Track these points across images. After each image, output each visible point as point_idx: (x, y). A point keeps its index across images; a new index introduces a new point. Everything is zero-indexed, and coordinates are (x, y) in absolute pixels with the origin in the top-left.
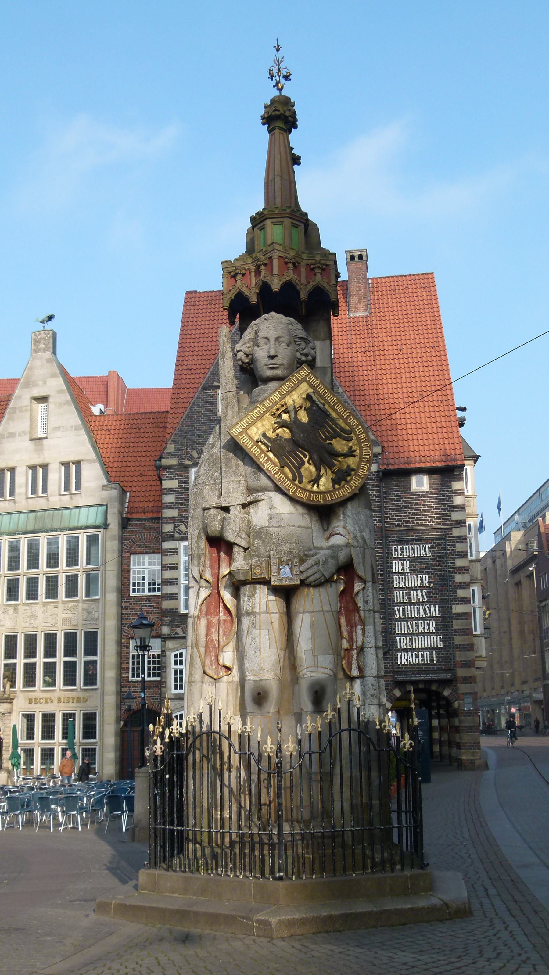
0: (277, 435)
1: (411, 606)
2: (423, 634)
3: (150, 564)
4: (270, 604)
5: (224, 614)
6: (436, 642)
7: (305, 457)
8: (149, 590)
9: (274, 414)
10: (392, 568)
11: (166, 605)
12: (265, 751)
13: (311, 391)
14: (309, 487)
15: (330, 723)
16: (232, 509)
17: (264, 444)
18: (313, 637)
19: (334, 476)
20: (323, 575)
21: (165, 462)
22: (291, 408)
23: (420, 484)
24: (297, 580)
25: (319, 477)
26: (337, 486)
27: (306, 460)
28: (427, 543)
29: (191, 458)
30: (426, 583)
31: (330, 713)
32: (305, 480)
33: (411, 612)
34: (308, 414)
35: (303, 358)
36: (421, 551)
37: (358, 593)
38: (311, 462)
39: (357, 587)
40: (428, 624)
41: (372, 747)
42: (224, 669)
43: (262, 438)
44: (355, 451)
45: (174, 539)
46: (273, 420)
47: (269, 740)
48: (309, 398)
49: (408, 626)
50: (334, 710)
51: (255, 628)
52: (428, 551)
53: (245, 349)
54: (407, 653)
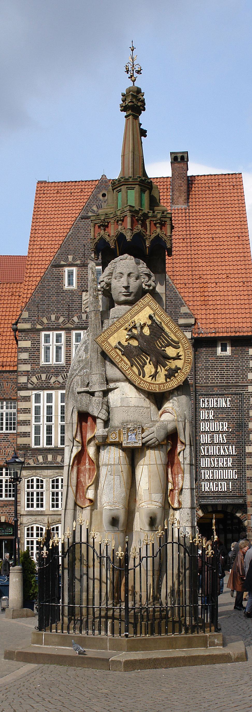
0: (129, 343)
1: (213, 446)
2: (222, 468)
3: (7, 408)
4: (121, 458)
5: (89, 464)
6: (232, 474)
7: (147, 359)
8: (7, 429)
9: (126, 329)
10: (200, 416)
11: (21, 441)
12: (117, 556)
13: (151, 313)
14: (149, 380)
15: (160, 538)
16: (96, 394)
17: (120, 349)
18: (149, 481)
19: (166, 373)
20: (158, 440)
21: (20, 326)
22: (138, 325)
23: (224, 349)
24: (140, 443)
25: (156, 373)
26: (168, 380)
27: (148, 361)
28: (228, 397)
29: (42, 323)
30: (225, 429)
31: (160, 532)
32: (147, 376)
33: (213, 450)
34: (150, 329)
35: (147, 288)
36: (222, 403)
37: (180, 453)
38: (151, 362)
39: (179, 448)
40: (227, 461)
41: (187, 554)
42: (88, 501)
43: (118, 345)
44: (181, 356)
45: (28, 389)
46: (126, 332)
47: (120, 549)
48: (150, 317)
49: (210, 462)
50: (163, 529)
51: (110, 475)
52: (228, 403)
53: (106, 280)
54: (210, 482)
